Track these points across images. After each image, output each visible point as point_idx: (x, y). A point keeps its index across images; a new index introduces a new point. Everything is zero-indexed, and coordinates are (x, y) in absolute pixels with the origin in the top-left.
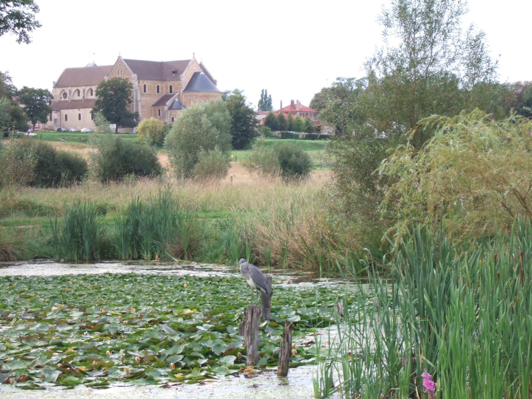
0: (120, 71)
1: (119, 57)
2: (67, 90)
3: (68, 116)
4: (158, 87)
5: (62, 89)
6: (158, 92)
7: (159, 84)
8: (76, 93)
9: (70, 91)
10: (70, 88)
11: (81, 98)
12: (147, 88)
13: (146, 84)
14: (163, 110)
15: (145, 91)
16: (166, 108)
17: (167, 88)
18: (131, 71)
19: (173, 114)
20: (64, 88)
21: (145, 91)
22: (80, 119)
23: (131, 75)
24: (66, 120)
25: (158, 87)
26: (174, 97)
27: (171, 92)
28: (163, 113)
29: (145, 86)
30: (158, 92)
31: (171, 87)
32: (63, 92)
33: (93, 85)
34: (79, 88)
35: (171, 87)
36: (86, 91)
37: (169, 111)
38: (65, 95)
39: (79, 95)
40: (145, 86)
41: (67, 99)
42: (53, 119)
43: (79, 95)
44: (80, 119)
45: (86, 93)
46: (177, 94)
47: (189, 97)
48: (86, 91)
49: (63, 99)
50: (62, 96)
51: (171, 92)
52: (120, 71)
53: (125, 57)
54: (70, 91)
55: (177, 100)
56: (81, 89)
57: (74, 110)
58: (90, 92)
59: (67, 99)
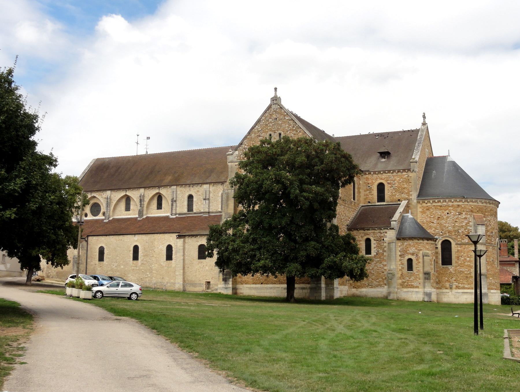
3: (106, 252)
6: (354, 199)
8: (123, 205)
9: (108, 201)
10: (109, 193)
11: (133, 214)
14: (380, 240)
16: (390, 235)
17: (370, 189)
19: (412, 250)
20: (94, 194)
22: (136, 257)
24: (101, 258)
26: (401, 209)
27: (381, 197)
28: (379, 246)
31: (381, 188)
33: (165, 186)
34: (129, 193)
35: (381, 188)
36: (147, 200)
37: (399, 243)
39: (128, 208)
41: (100, 217)
43: (128, 208)
44: (136, 257)
45: (146, 203)
46: (404, 203)
47: (439, 212)
48: (147, 200)
51: (381, 197)
54: (108, 201)
55: (410, 216)
56: (134, 195)
57: (121, 237)
58: (155, 202)
59: (100, 217)
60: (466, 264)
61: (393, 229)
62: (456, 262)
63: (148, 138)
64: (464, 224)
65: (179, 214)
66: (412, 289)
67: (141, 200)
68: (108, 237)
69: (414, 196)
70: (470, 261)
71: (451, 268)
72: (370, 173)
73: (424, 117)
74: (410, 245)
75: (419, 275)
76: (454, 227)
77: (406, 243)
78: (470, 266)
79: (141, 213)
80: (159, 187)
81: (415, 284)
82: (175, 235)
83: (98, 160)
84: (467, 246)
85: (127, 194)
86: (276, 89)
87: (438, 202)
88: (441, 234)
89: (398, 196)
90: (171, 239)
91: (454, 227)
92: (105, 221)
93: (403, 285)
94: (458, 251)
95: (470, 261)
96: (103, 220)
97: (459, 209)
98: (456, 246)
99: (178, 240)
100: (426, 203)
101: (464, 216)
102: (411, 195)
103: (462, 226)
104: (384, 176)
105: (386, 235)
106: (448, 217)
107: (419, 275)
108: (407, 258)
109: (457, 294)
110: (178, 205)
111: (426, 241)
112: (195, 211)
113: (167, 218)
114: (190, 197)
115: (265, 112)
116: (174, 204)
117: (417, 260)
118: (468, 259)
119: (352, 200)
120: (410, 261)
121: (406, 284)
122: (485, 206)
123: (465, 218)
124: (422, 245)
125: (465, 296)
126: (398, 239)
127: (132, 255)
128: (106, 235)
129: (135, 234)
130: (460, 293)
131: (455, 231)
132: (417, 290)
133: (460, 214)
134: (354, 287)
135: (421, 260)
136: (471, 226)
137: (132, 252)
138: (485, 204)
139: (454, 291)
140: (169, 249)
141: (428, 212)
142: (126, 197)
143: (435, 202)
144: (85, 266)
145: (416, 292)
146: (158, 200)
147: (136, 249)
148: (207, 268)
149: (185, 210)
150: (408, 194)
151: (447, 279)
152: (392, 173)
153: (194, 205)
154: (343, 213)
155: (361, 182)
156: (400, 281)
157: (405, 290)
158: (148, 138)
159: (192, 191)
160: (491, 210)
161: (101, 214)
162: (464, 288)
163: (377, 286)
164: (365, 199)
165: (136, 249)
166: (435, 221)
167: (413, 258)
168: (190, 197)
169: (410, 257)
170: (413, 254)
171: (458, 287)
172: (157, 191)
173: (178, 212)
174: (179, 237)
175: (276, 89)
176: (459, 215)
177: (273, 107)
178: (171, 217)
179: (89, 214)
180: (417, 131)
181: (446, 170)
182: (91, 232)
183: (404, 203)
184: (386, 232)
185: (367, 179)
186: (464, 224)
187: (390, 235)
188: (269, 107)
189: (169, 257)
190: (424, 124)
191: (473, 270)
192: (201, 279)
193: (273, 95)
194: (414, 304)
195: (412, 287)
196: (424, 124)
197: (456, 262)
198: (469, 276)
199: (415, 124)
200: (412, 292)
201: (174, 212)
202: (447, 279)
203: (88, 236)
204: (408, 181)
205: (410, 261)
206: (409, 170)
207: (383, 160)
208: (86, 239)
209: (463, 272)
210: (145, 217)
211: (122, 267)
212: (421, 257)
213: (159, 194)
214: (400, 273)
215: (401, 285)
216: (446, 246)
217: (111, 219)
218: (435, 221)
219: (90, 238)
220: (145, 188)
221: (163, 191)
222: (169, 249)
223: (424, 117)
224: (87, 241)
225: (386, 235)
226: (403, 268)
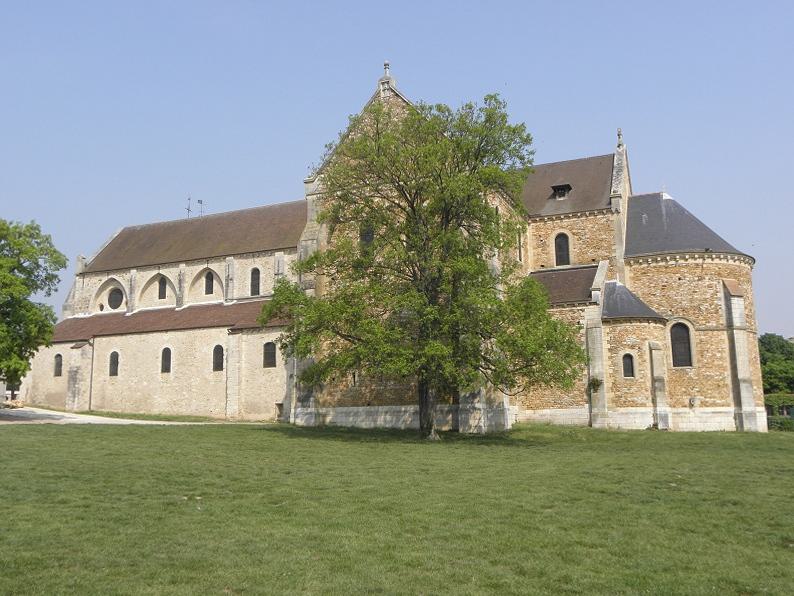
2: (123, 279)
3: (121, 360)
5: (105, 279)
10: (134, 271)
11: (169, 303)
19: (631, 339)
22: (166, 368)
31: (562, 241)
35: (562, 241)
36: (189, 280)
37: (606, 329)
38: (116, 297)
41: (122, 309)
42: (65, 369)
44: (166, 368)
48: (189, 280)
49: (108, 310)
50: (104, 299)
56: (170, 273)
57: (144, 336)
60: (716, 363)
61: (595, 303)
62: (699, 361)
64: (708, 296)
65: (238, 300)
66: (634, 408)
67: (180, 280)
69: (620, 251)
70: (721, 358)
71: (691, 372)
72: (542, 220)
74: (627, 330)
75: (644, 382)
76: (691, 301)
77: (620, 327)
78: (720, 367)
79: (179, 301)
80: (208, 259)
81: (639, 399)
82: (225, 330)
84: (715, 333)
85: (161, 272)
87: (662, 260)
88: (670, 313)
89: (591, 254)
90: (220, 336)
91: (691, 301)
92: (128, 314)
93: (618, 402)
94: (701, 341)
95: (721, 358)
96: (125, 313)
97: (698, 271)
98: (697, 333)
99: (231, 336)
100: (641, 264)
101: (707, 282)
102: (615, 251)
103: (706, 299)
104: (566, 222)
105: (582, 314)
106: (680, 285)
107: (644, 382)
108: (622, 353)
109: (704, 415)
110: (236, 285)
111: (653, 324)
112: (261, 294)
113: (220, 305)
114: (256, 273)
116: (230, 285)
117: (641, 356)
118: (719, 355)
120: (628, 358)
121: (623, 399)
122: (739, 267)
123: (710, 286)
124: (647, 330)
125: (718, 418)
126: (605, 321)
127: (160, 365)
128: (122, 334)
129: (167, 331)
130: (708, 413)
131: (694, 308)
132: (643, 409)
133: (701, 279)
134: (529, 408)
135: (647, 357)
136: (720, 299)
137: (160, 359)
138: (737, 263)
139: (698, 410)
140: (219, 351)
141: (645, 279)
142: (159, 278)
143: (657, 261)
145: (642, 413)
146: (207, 282)
147: (167, 353)
148: (278, 381)
149: (248, 293)
150: (609, 248)
151: (684, 389)
153: (261, 284)
156: (612, 395)
157: (622, 410)
159: (258, 263)
162: (714, 404)
163: (571, 404)
164: (536, 261)
165: (167, 353)
166: (658, 293)
167: (633, 353)
168: (256, 273)
169: (628, 351)
170: (632, 347)
171: (704, 404)
172: (205, 266)
173: (235, 297)
174: (234, 331)
176: (699, 280)
178: (226, 304)
181: (664, 212)
183: (603, 265)
184: (583, 311)
186: (708, 296)
187: (591, 314)
189: (218, 365)
191: (728, 373)
192: (268, 399)
194: (635, 434)
195: (635, 404)
197: (699, 361)
198: (721, 383)
200: (636, 413)
201: (229, 297)
202: (684, 389)
204: (608, 228)
205: (628, 358)
208: (91, 341)
209: (712, 377)
210: (185, 306)
211: (145, 383)
212: (648, 352)
213: (206, 273)
214: (612, 380)
215: (613, 401)
216: (680, 334)
218: (658, 293)
219: (97, 340)
220: (188, 262)
221: (214, 266)
222: (219, 351)
224: (92, 345)
225: (582, 314)
226: (616, 371)
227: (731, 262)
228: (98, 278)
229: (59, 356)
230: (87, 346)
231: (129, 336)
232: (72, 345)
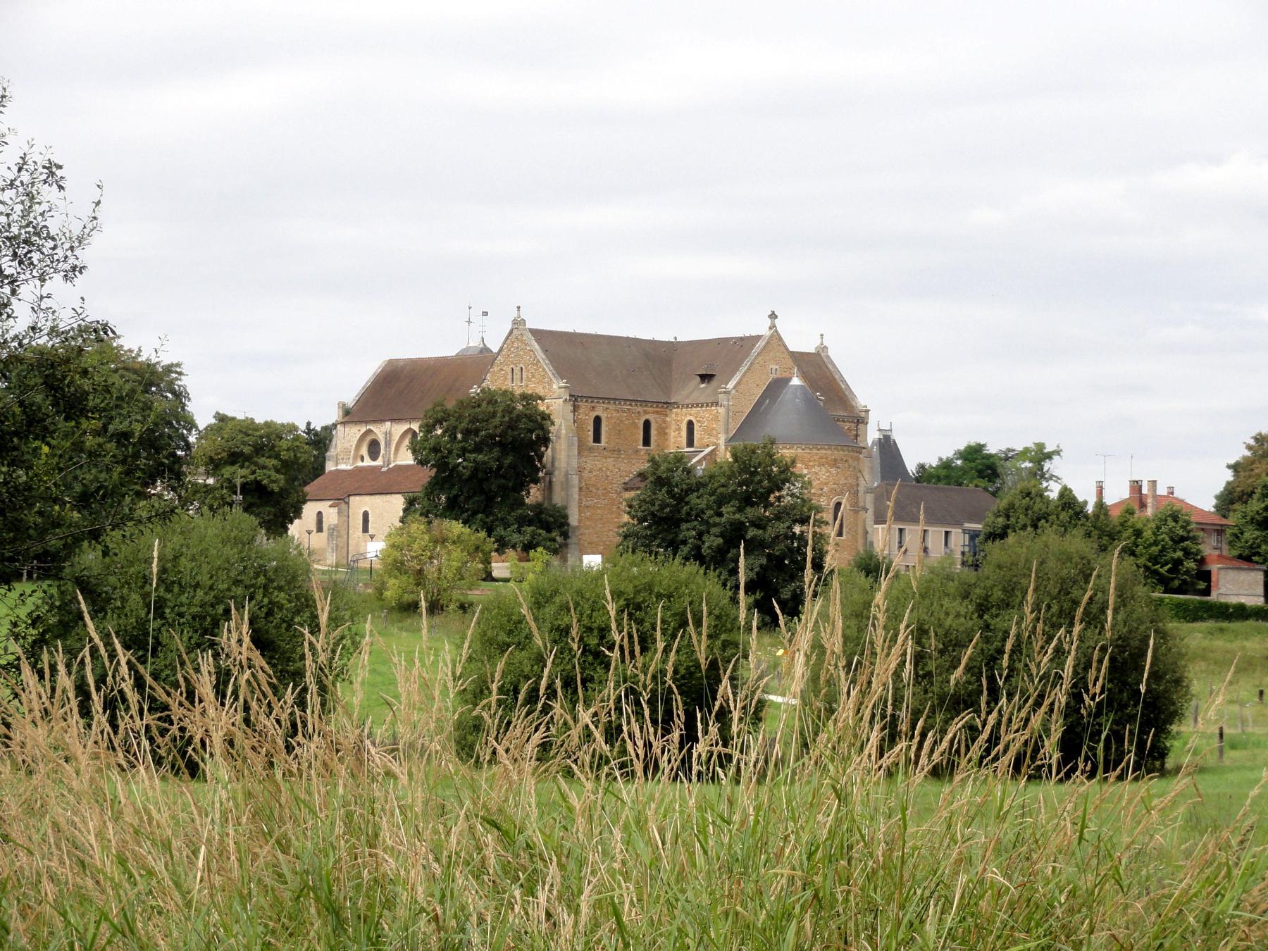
0: (517, 370)
1: (518, 323)
2: (379, 431)
3: (371, 518)
4: (647, 425)
7: (651, 417)
9: (388, 435)
10: (388, 424)
12: (604, 429)
13: (603, 416)
15: (597, 438)
17: (679, 429)
18: (549, 369)
20: (370, 427)
21: (597, 438)
23: (550, 384)
25: (647, 425)
29: (598, 421)
30: (647, 442)
32: (369, 438)
35: (690, 425)
40: (598, 421)
41: (379, 462)
42: (325, 526)
49: (368, 462)
50: (364, 451)
52: (517, 370)
53: (536, 322)
54: (388, 435)
57: (388, 497)
59: (379, 462)
63: (485, 314)
68: (372, 497)
73: (773, 316)
83: (390, 362)
86: (519, 308)
92: (383, 470)
104: (694, 410)
115: (507, 338)
119: (641, 447)
128: (371, 494)
144: (345, 540)
152: (702, 406)
154: (610, 468)
155: (668, 419)
158: (485, 314)
160: (821, 458)
161: (380, 458)
164: (674, 443)
175: (519, 308)
177: (515, 332)
179: (367, 457)
180: (759, 337)
182: (356, 489)
185: (677, 415)
188: (511, 332)
190: (773, 327)
193: (515, 315)
196: (773, 327)
199: (760, 327)
203: (349, 496)
204: (716, 419)
206: (717, 404)
207: (703, 385)
217: (391, 466)
219: (352, 498)
223: (773, 316)
224: (348, 503)
227: (800, 451)
228: (358, 427)
229: (320, 514)
230: (344, 506)
231: (377, 497)
232: (330, 503)
